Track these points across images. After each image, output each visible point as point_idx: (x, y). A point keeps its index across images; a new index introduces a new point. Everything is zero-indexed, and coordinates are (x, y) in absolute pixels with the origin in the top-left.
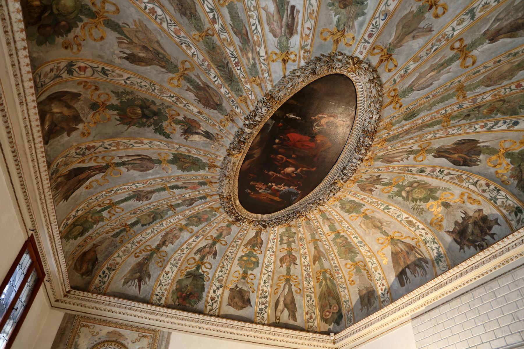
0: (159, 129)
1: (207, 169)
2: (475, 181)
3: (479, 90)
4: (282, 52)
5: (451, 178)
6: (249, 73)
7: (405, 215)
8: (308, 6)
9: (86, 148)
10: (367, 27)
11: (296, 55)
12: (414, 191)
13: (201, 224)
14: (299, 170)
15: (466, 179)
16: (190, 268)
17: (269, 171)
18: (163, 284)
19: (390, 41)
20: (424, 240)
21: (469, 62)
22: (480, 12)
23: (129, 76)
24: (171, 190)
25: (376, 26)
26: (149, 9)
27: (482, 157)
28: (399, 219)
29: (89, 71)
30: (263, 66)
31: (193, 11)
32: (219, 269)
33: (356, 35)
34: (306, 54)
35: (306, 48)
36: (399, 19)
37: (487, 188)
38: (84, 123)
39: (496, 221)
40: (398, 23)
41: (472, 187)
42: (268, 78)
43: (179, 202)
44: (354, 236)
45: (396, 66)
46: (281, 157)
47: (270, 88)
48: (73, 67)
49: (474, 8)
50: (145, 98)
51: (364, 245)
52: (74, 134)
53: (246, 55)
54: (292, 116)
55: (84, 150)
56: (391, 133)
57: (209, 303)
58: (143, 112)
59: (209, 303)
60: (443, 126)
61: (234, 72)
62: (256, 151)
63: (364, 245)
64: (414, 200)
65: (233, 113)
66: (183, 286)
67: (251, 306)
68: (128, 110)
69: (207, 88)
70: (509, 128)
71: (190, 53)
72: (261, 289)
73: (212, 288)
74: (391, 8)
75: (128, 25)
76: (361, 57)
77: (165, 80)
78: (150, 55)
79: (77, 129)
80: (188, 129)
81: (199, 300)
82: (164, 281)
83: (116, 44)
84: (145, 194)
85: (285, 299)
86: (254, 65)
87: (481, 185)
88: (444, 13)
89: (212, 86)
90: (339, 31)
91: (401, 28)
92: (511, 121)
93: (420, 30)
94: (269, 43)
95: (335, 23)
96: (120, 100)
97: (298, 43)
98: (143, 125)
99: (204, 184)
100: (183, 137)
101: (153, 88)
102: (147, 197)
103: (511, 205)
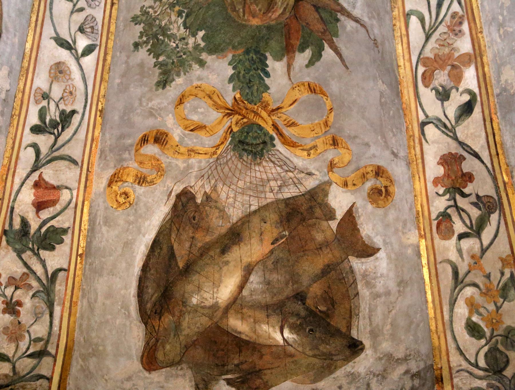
38: (329, 183)
48: (34, 226)
52: (369, 229)
55: (462, 203)
68: (255, 22)
79: (350, 215)
96: (204, 56)
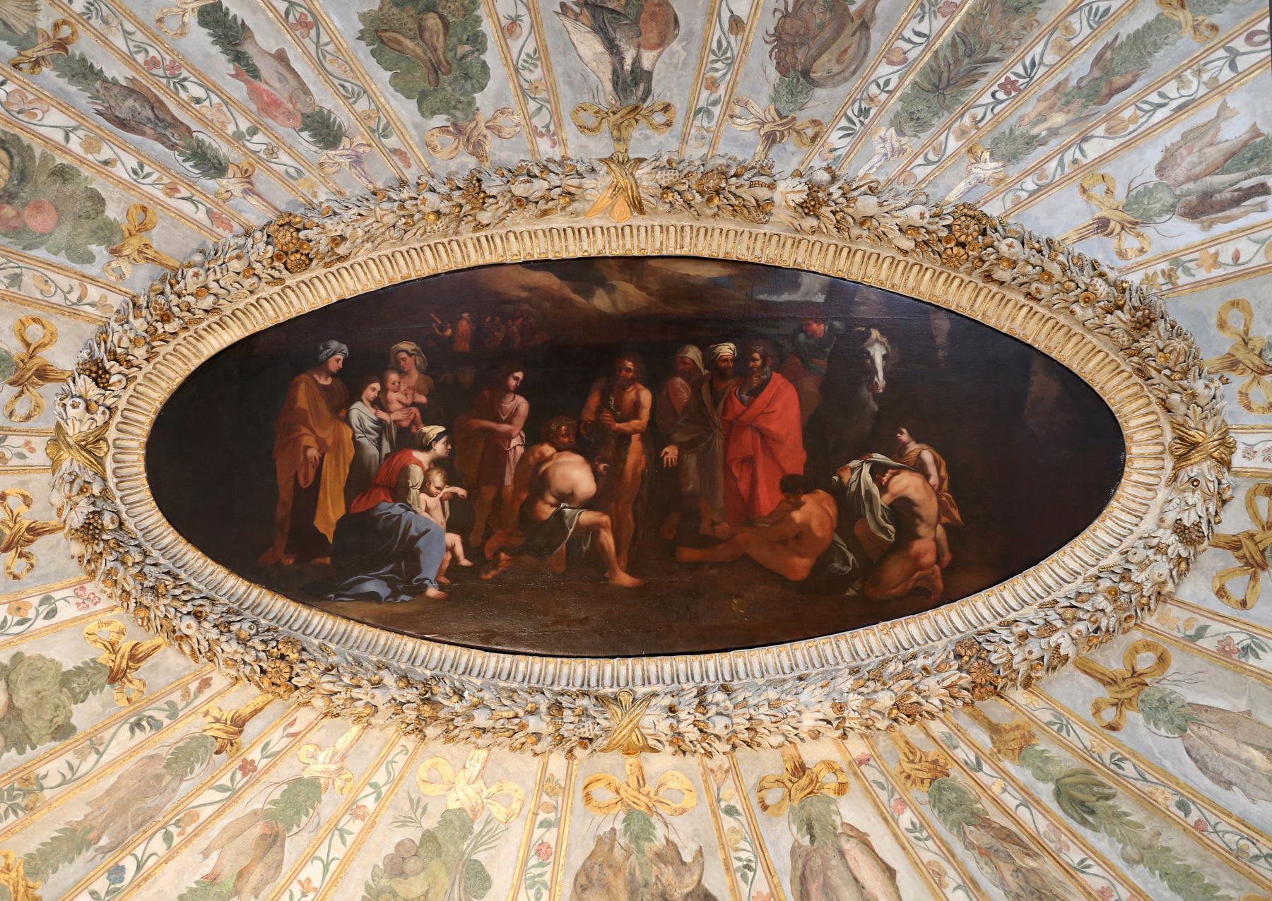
4: (1127, 207)
6: (996, 134)
11: (1142, 251)
14: (587, 517)
17: (521, 390)
30: (1053, 164)
34: (1161, 280)
35: (1180, 272)
42: (1024, 195)
45: (1244, 604)
46: (637, 405)
53: (1051, 108)
54: (878, 353)
56: (987, 775)
61: (978, 86)
62: (631, 289)
65: (810, 132)
80: (613, 11)
86: (1032, 142)
89: (875, 35)
94: (1130, 157)
97: (1180, 243)
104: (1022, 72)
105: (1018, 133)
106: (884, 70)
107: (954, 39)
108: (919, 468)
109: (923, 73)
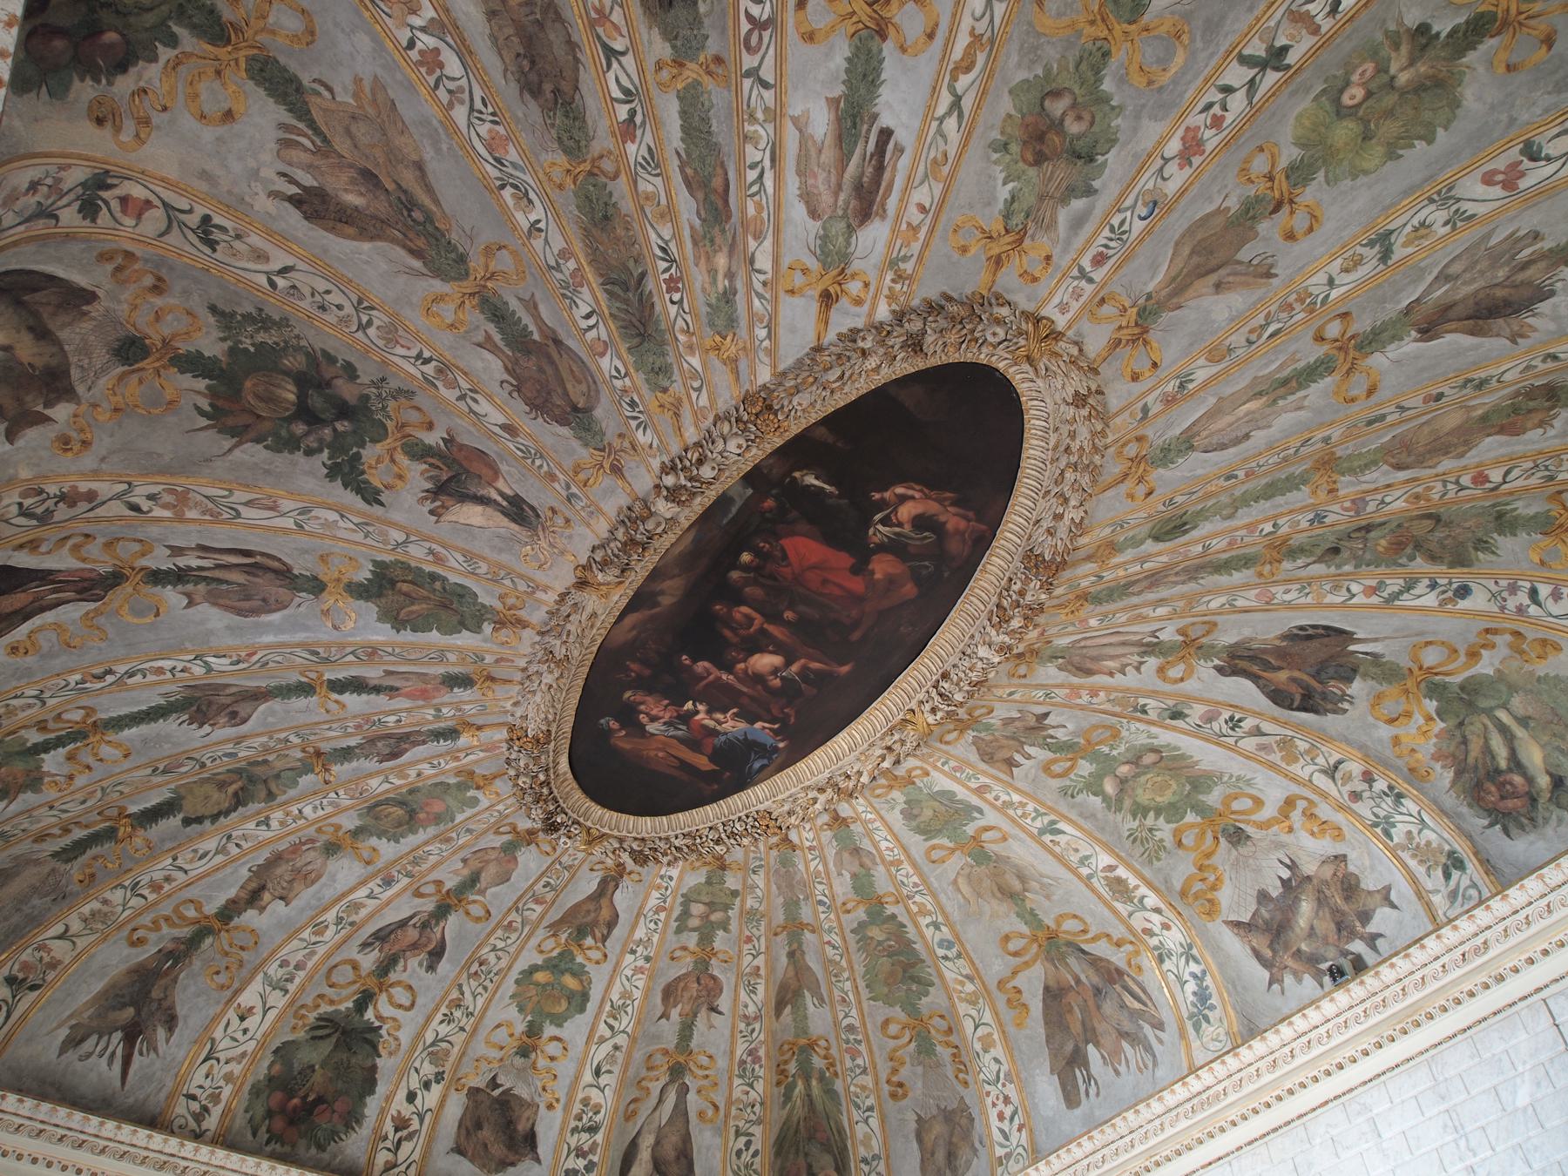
0: (346, 470)
1: (487, 628)
2: (1332, 762)
3: (1375, 475)
5: (1262, 747)
6: (705, 320)
7: (1105, 859)
8: (934, 138)
9: (62, 497)
10: (1096, 233)
11: (866, 285)
12: (1143, 779)
13: (415, 832)
14: (795, 668)
15: (1308, 752)
16: (332, 1002)
17: (695, 661)
18: (222, 1056)
19: (1150, 287)
20: (1156, 948)
21: (1358, 386)
22: (1405, 245)
23: (290, 261)
24: (335, 696)
25: (1119, 233)
26: (421, 52)
27: (1357, 687)
28: (1085, 871)
29: (154, 220)
30: (756, 302)
31: (565, 86)
32: (444, 1010)
33: (1056, 252)
34: (898, 287)
36: (1186, 226)
37: (1366, 786)
38: (79, 403)
39: (1386, 897)
40: (1183, 236)
41: (1321, 781)
42: (766, 343)
43: (353, 742)
44: (928, 920)
45: (1155, 365)
46: (746, 616)
47: (764, 376)
48: (105, 194)
49: (1392, 232)
50: (324, 352)
51: (959, 956)
52: (32, 436)
54: (811, 480)
55: (50, 503)
57: (386, 1138)
58: (302, 397)
59: (386, 1138)
60: (1261, 575)
61: (658, 308)
62: (668, 583)
63: (959, 956)
64: (1140, 811)
65: (626, 444)
66: (297, 1067)
67: (538, 1160)
68: (248, 384)
69: (553, 350)
70: (1443, 603)
71: (523, 221)
72: (580, 1096)
73: (404, 1083)
74: (1171, 188)
75: (330, 90)
76: (1061, 322)
77: (415, 300)
78: (381, 207)
79: (48, 419)
80: (450, 480)
81: (349, 1127)
82: (226, 1043)
83: (273, 146)
84: (228, 700)
85: (658, 1143)
86: (728, 297)
87: (1348, 778)
88: (1311, 230)
89: (571, 343)
90: (1007, 231)
91: (1186, 251)
92: (1450, 583)
93: (1239, 268)
94: (788, 233)
95: (1001, 205)
96: (229, 343)
97: (880, 248)
98: (290, 444)
99: (465, 681)
100: (429, 505)
101: (365, 319)
102: (234, 715)
103: (1434, 845)
104: (666, 265)
105: (714, 301)
106: (605, 363)
107: (606, 291)
108: (903, 499)
109: (624, 337)
